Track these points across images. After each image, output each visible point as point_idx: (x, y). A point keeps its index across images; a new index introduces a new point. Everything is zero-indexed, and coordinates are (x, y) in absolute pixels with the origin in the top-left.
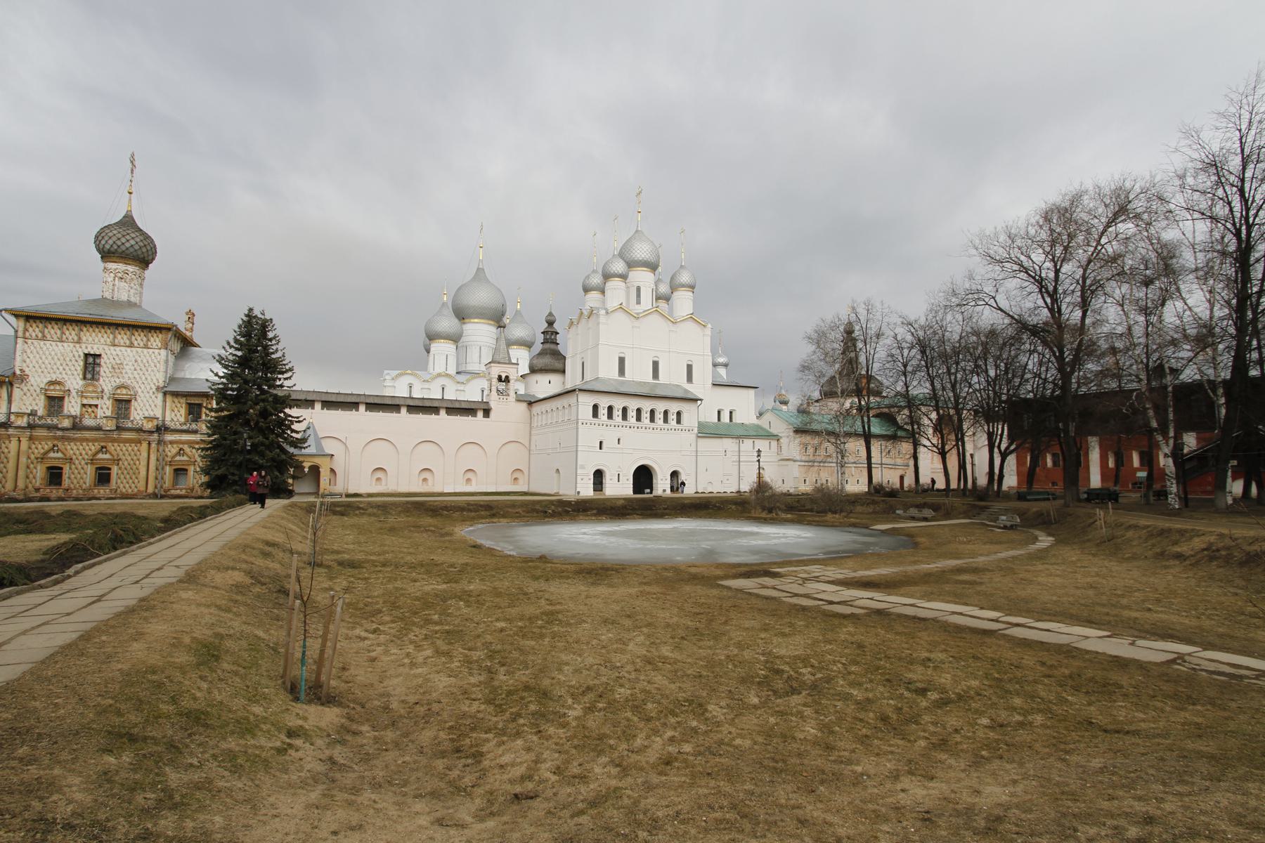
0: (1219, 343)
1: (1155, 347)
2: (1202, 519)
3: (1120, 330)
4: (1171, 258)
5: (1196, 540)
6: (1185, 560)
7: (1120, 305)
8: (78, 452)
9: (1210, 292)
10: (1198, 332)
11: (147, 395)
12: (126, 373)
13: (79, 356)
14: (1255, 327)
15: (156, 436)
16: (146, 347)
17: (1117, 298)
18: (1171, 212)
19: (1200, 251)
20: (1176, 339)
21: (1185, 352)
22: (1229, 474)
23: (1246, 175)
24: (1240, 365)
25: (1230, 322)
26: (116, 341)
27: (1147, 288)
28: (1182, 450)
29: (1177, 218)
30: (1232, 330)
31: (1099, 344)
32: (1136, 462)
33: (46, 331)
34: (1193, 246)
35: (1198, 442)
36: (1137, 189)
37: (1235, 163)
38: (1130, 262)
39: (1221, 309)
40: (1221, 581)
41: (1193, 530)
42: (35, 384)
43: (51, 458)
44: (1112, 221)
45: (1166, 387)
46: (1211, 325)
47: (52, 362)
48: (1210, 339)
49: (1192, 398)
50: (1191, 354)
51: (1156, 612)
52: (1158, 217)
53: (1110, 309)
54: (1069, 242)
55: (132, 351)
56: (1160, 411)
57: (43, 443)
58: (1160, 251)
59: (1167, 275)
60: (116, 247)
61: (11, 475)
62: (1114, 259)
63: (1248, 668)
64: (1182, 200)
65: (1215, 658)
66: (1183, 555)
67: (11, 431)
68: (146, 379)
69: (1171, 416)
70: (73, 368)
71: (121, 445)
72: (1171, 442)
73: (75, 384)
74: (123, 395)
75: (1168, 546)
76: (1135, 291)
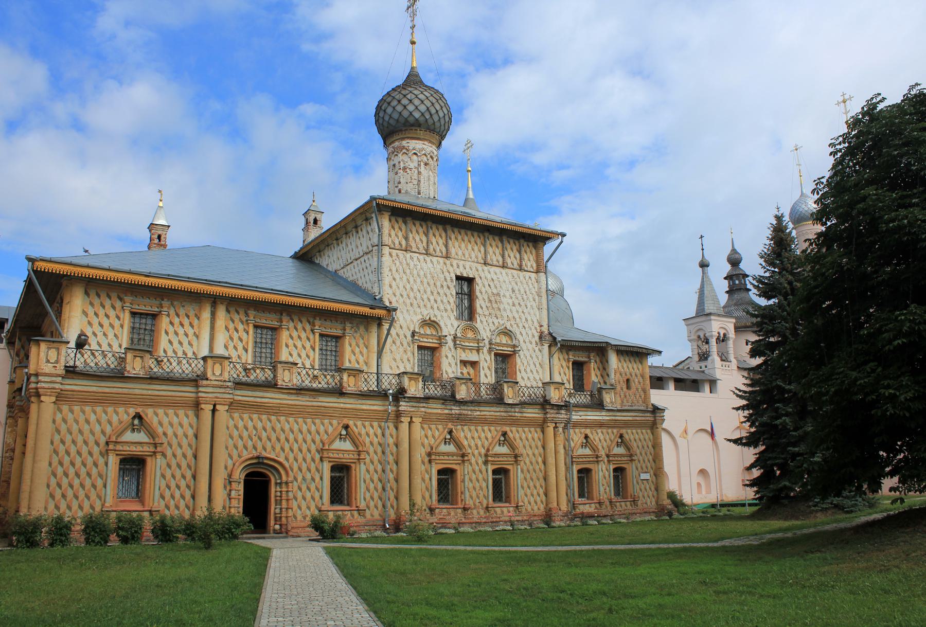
8: (473, 444)
11: (530, 347)
12: (505, 310)
13: (452, 280)
15: (563, 415)
16: (521, 269)
26: (489, 256)
33: (411, 236)
42: (404, 326)
43: (444, 454)
47: (422, 289)
55: (507, 275)
57: (433, 427)
60: (428, 116)
61: (405, 483)
67: (404, 406)
68: (527, 320)
70: (445, 301)
71: (520, 429)
73: (449, 326)
74: (504, 345)
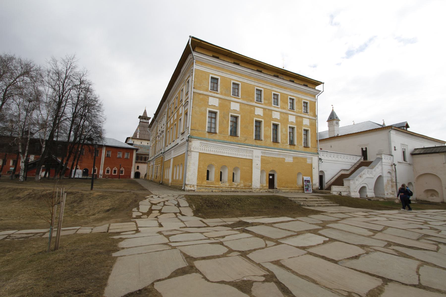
0: (47, 128)
1: (27, 124)
2: (30, 184)
3: (16, 114)
4: (40, 96)
5: (26, 192)
6: (20, 199)
7: (18, 105)
9: (49, 111)
10: (42, 123)
14: (58, 126)
17: (18, 102)
18: (43, 81)
19: (49, 97)
20: (35, 123)
21: (37, 128)
22: (41, 169)
23: (65, 81)
24: (52, 136)
25: (52, 122)
27: (29, 103)
28: (29, 160)
29: (44, 84)
30: (52, 125)
31: (6, 117)
32: (11, 164)
34: (47, 95)
35: (34, 159)
36: (34, 68)
37: (64, 76)
38: (25, 91)
39: (50, 117)
40: (31, 205)
41: (25, 188)
44: (23, 74)
45: (27, 138)
46: (46, 122)
48: (45, 126)
49: (36, 144)
50: (38, 129)
51: (4, 220)
52: (39, 81)
53: (14, 105)
54: (3, 74)
56: (24, 146)
58: (36, 92)
59: (37, 101)
62: (20, 88)
63: (32, 233)
64: (47, 79)
65: (21, 233)
66: (20, 197)
69: (27, 149)
72: (25, 158)
75: (15, 195)
76: (25, 102)
